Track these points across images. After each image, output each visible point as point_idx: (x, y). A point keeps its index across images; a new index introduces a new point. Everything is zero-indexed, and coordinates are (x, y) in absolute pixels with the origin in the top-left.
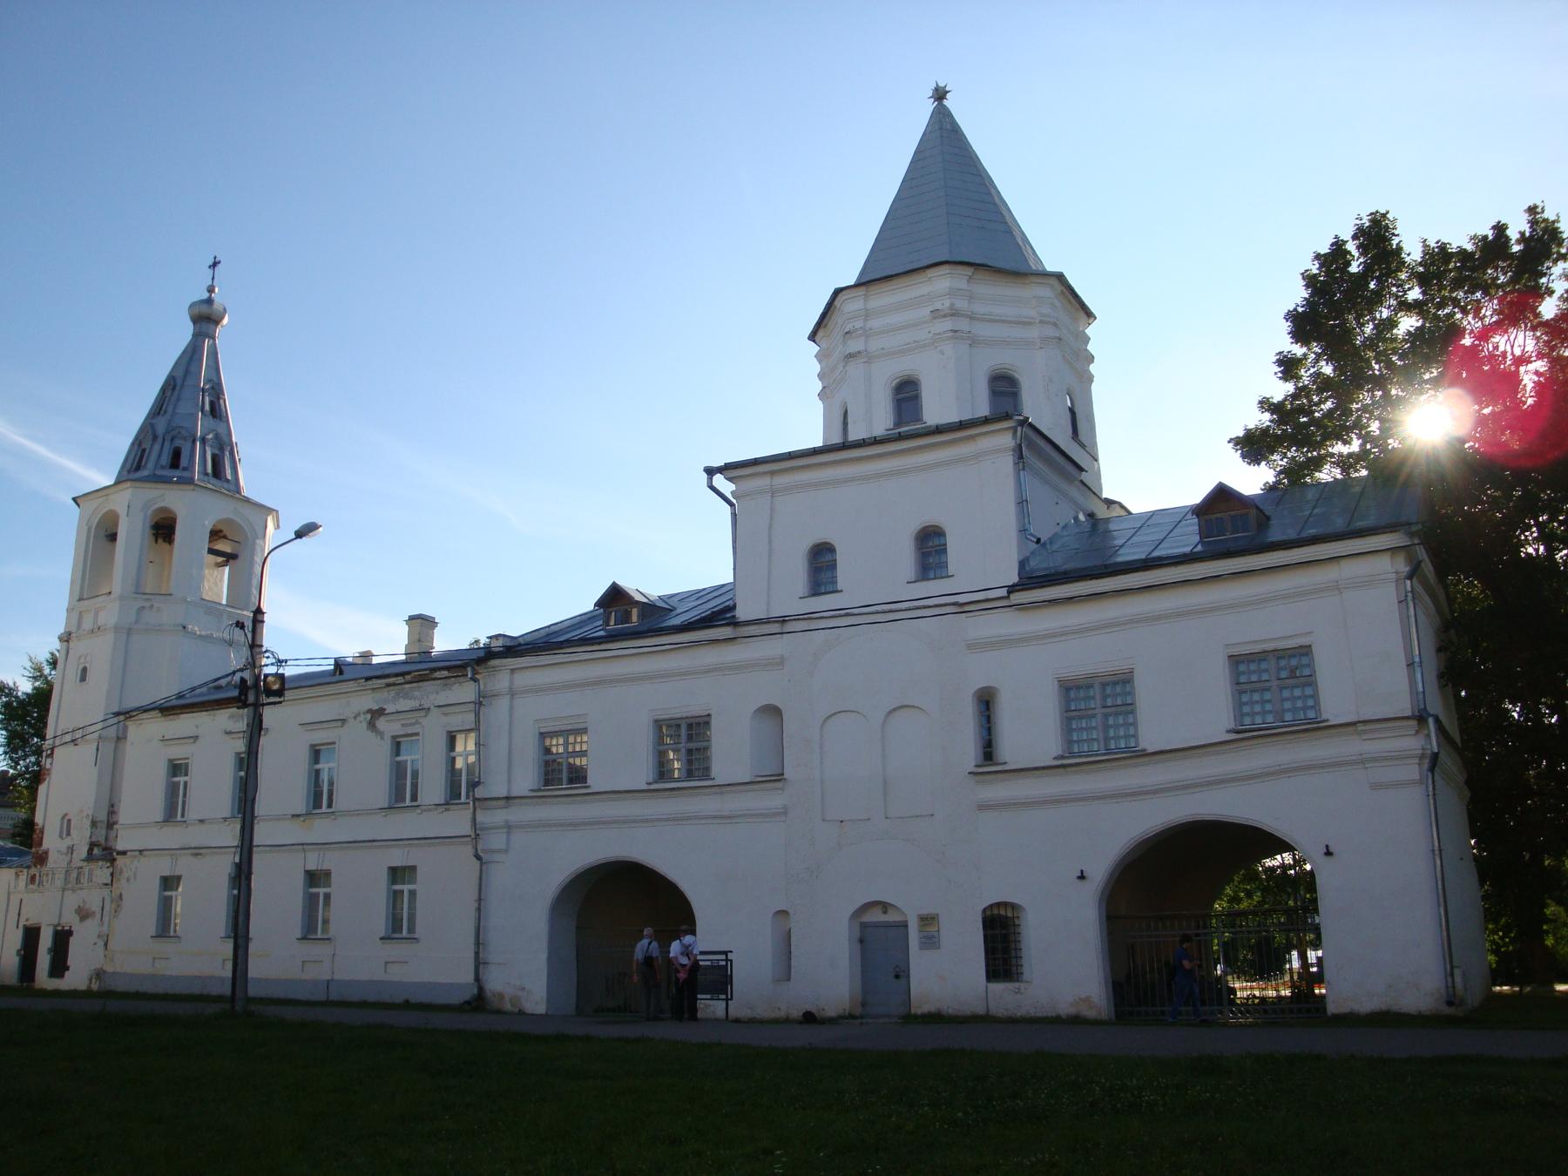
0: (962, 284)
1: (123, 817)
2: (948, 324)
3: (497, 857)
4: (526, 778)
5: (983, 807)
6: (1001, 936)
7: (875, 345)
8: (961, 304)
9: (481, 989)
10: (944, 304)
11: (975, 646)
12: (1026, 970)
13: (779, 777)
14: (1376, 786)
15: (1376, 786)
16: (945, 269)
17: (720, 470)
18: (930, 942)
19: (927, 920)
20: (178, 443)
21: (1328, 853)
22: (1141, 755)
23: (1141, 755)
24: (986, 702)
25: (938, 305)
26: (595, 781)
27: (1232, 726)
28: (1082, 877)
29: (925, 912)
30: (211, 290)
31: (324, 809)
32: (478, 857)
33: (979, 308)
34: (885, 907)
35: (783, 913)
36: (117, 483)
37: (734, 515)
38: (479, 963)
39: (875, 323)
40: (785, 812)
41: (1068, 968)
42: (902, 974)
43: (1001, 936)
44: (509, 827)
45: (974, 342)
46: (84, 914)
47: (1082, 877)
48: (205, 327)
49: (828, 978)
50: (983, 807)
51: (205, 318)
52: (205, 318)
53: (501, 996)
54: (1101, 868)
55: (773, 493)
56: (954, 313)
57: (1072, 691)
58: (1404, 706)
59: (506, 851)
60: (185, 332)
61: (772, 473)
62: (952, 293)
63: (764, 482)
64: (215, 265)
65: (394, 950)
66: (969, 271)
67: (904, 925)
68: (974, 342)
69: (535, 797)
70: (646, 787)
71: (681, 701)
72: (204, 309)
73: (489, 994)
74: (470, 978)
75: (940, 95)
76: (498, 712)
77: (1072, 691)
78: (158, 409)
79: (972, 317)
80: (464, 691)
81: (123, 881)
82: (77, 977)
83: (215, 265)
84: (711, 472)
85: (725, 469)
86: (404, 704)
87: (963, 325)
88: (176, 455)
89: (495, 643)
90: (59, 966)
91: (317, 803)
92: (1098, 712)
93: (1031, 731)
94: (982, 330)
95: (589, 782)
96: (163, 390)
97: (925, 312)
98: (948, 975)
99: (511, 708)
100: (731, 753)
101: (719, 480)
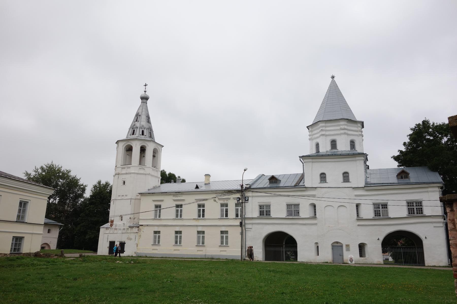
0: (346, 123)
4: (256, 214)
5: (358, 225)
7: (328, 133)
8: (346, 127)
14: (434, 227)
15: (434, 227)
19: (348, 246)
22: (390, 218)
24: (358, 206)
25: (341, 127)
26: (273, 215)
28: (379, 239)
29: (347, 244)
30: (145, 92)
31: (201, 217)
33: (349, 128)
34: (337, 242)
35: (317, 243)
41: (376, 256)
42: (342, 255)
44: (252, 224)
45: (348, 134)
46: (130, 239)
47: (379, 239)
48: (145, 101)
49: (326, 256)
50: (358, 225)
54: (382, 239)
61: (312, 159)
63: (311, 160)
66: (347, 120)
67: (342, 246)
68: (348, 134)
70: (284, 217)
75: (333, 77)
81: (142, 232)
83: (146, 85)
84: (300, 157)
87: (346, 131)
88: (143, 132)
92: (381, 210)
93: (368, 211)
95: (271, 215)
97: (338, 128)
98: (351, 256)
100: (305, 211)
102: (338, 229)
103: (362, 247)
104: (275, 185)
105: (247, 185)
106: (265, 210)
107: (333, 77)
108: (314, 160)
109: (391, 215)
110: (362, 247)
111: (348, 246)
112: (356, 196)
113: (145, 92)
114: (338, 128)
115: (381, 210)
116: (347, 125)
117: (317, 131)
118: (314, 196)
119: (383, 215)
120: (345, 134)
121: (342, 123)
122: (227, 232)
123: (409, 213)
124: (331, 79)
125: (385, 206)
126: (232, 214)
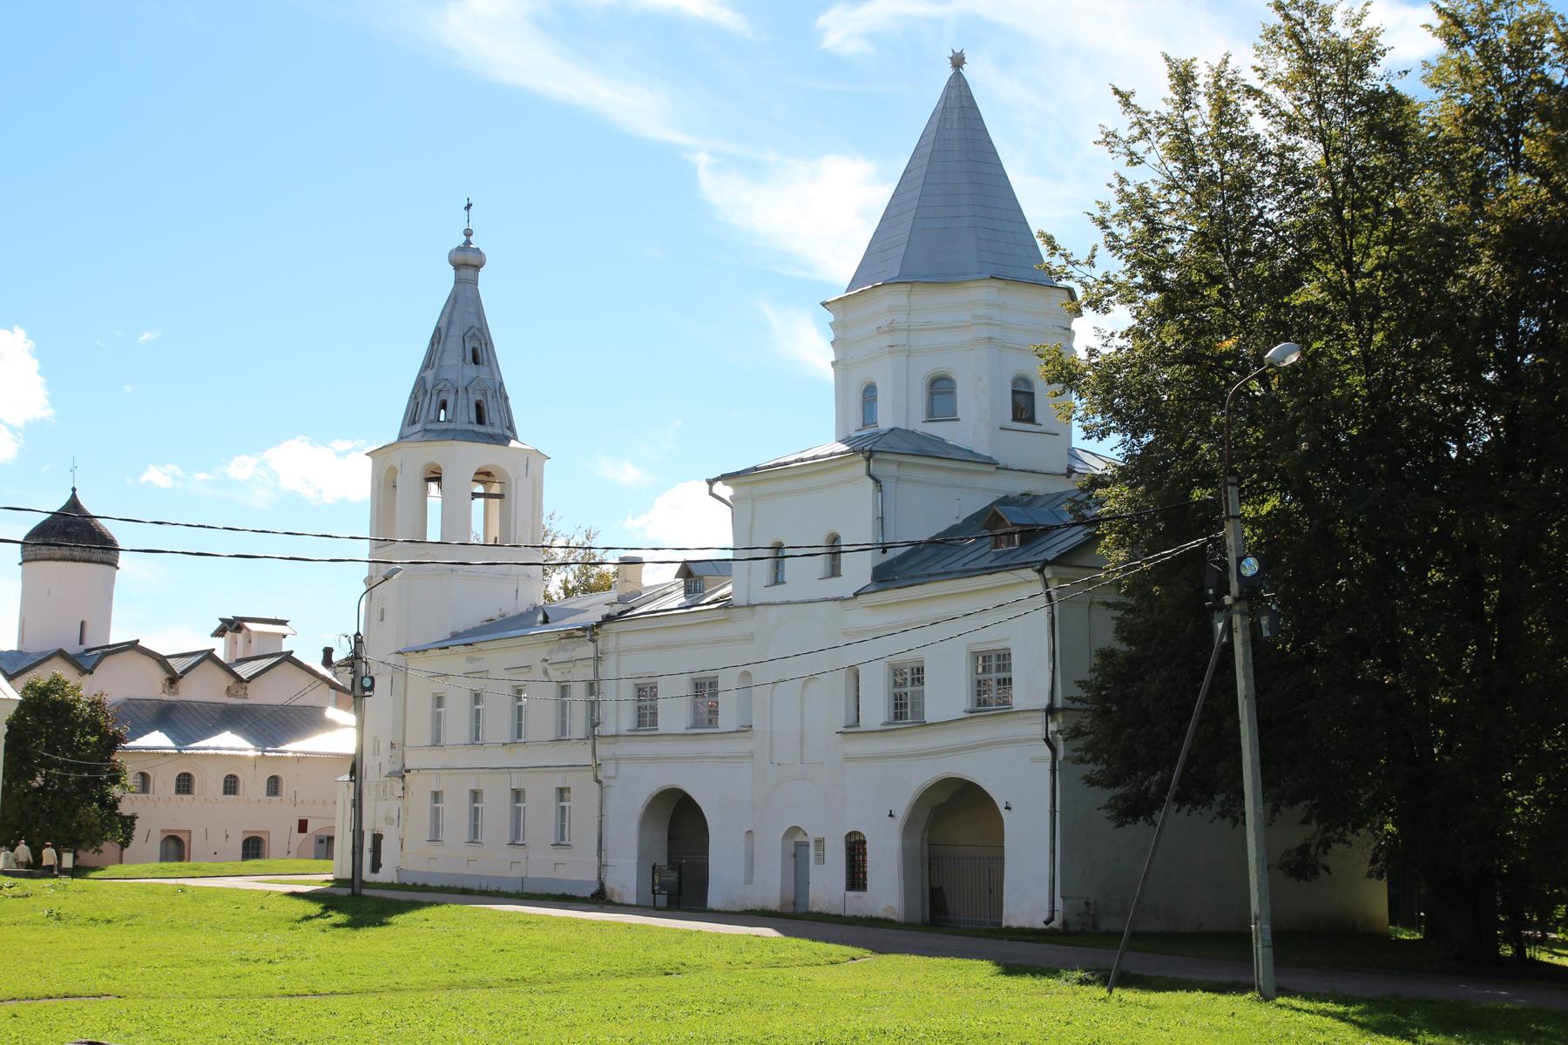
1: (408, 743)
2: (887, 340)
4: (627, 721)
5: (848, 759)
9: (602, 885)
12: (869, 883)
13: (746, 729)
17: (717, 479)
18: (821, 859)
19: (820, 842)
20: (443, 396)
23: (925, 724)
27: (969, 707)
29: (819, 836)
30: (468, 233)
35: (749, 832)
36: (401, 438)
38: (602, 867)
44: (617, 760)
50: (848, 759)
51: (467, 263)
52: (467, 263)
53: (613, 891)
54: (902, 811)
56: (892, 329)
58: (1044, 702)
60: (446, 279)
64: (468, 207)
65: (560, 855)
67: (807, 845)
69: (632, 735)
72: (461, 258)
73: (608, 891)
74: (595, 878)
75: (958, 61)
76: (608, 669)
78: (428, 364)
80: (587, 650)
82: (386, 875)
83: (468, 207)
84: (711, 482)
85: (725, 478)
86: (562, 656)
90: (376, 866)
92: (906, 689)
96: (432, 344)
99: (618, 663)
101: (719, 488)
103: (856, 848)
110: (856, 848)
111: (820, 842)
113: (468, 233)
115: (906, 689)
118: (751, 638)
126: (578, 727)
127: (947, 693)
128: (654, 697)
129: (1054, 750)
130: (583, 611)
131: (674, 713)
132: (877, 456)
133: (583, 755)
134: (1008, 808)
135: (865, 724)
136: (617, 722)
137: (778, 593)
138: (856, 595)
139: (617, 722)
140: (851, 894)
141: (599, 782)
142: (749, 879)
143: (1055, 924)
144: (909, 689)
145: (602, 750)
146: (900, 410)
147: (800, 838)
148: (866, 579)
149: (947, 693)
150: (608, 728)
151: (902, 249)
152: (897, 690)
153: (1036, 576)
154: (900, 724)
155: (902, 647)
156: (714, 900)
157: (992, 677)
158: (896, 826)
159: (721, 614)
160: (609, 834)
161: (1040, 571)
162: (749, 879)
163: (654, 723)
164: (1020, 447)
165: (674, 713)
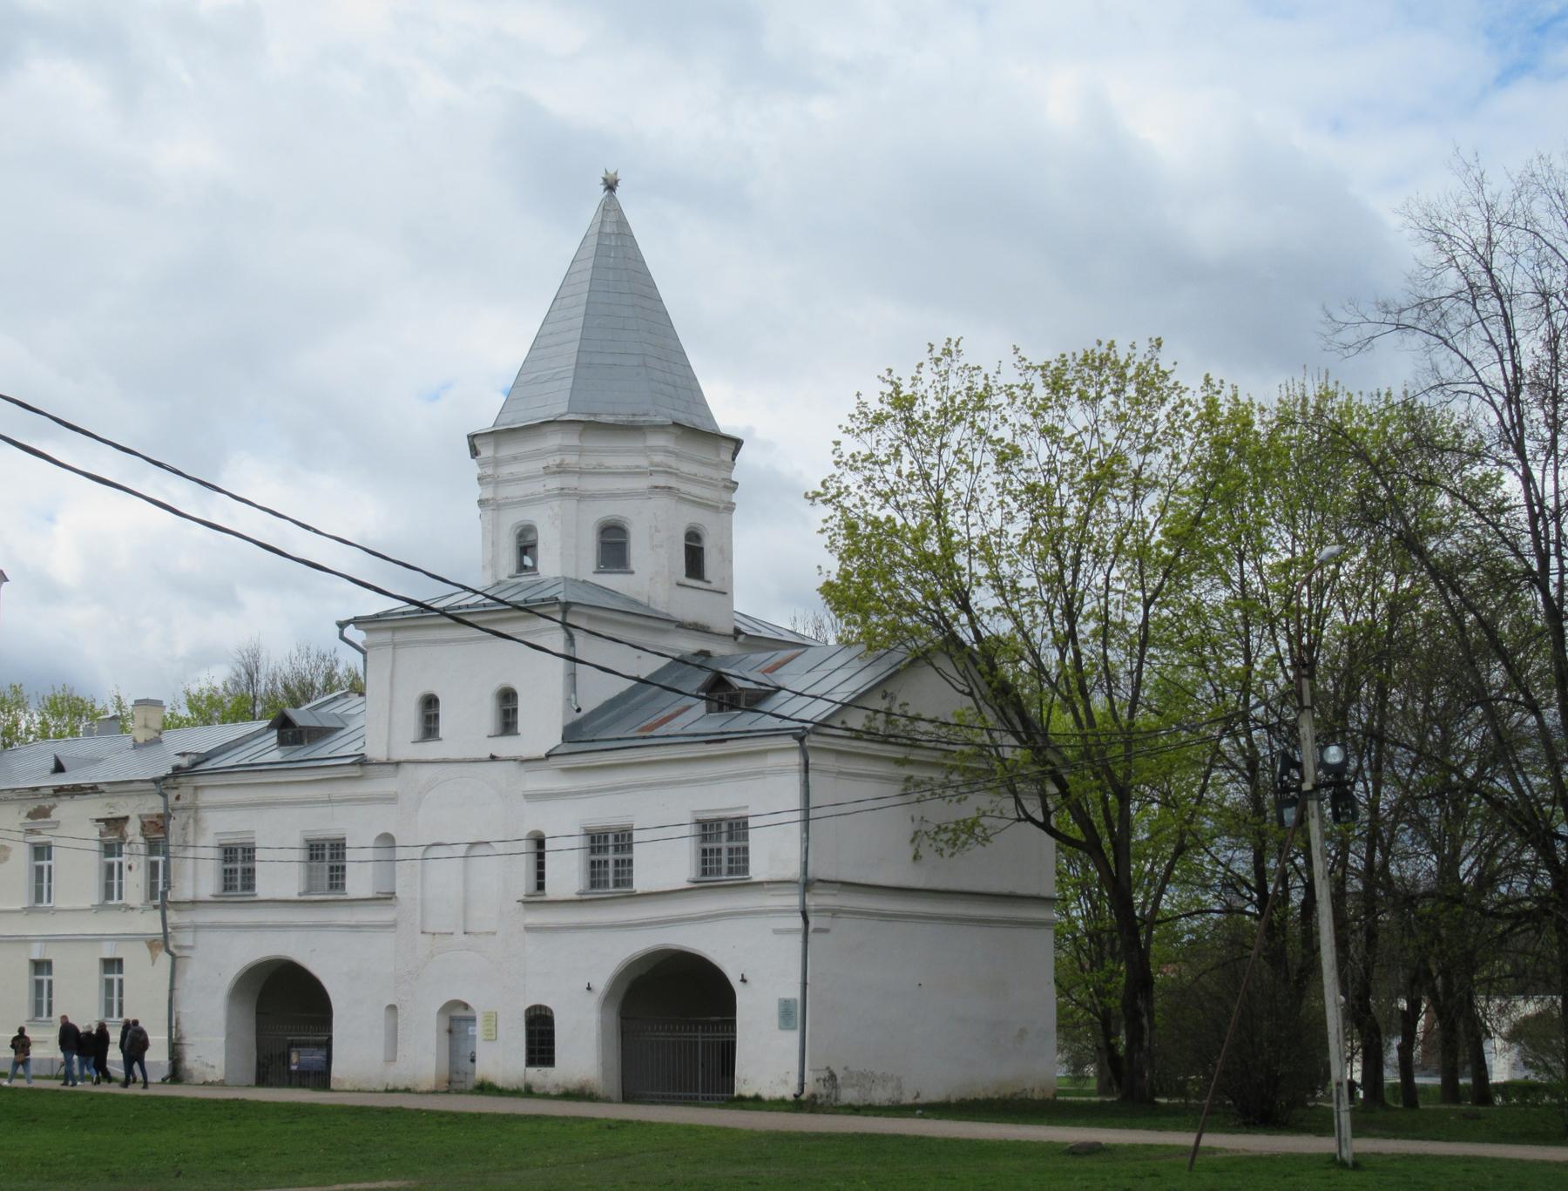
2: (554, 483)
3: (186, 953)
6: (540, 1035)
8: (571, 459)
10: (553, 461)
11: (530, 797)
13: (387, 898)
14: (776, 932)
15: (776, 932)
16: (557, 427)
17: (348, 622)
18: (492, 1037)
21: (744, 980)
32: (168, 951)
33: (590, 461)
35: (392, 1008)
37: (365, 661)
39: (505, 471)
40: (392, 925)
43: (540, 1035)
44: (196, 928)
45: (581, 497)
49: (421, 1061)
54: (601, 982)
55: (395, 645)
56: (561, 470)
57: (597, 840)
58: (793, 870)
59: (191, 948)
61: (394, 629)
62: (561, 450)
63: (386, 637)
67: (473, 1020)
68: (581, 497)
70: (295, 897)
71: (325, 824)
75: (611, 186)
77: (597, 840)
79: (581, 473)
84: (342, 625)
85: (357, 621)
87: (571, 482)
89: (184, 762)
91: (39, 898)
93: (567, 873)
94: (591, 484)
97: (537, 466)
101: (351, 632)
102: (462, 950)
104: (301, 753)
105: (183, 754)
106: (239, 866)
107: (611, 186)
108: (400, 637)
109: (640, 883)
111: (492, 1018)
112: (530, 797)
114: (537, 466)
116: (581, 452)
117: (527, 462)
118: (391, 799)
119: (617, 884)
120: (562, 493)
121: (554, 440)
122: (120, 961)
123: (704, 872)
124: (600, 193)
125: (623, 839)
127: (664, 862)
128: (252, 859)
129: (806, 922)
130: (95, 761)
131: (280, 876)
132: (574, 608)
133: (150, 923)
134: (744, 980)
135: (553, 890)
136: (195, 886)
137: (431, 750)
138: (548, 756)
139: (195, 886)
140: (533, 1071)
141: (172, 954)
142: (391, 1057)
143: (804, 1097)
144: (611, 857)
145: (173, 917)
146: (564, 558)
147: (461, 1013)
148: (554, 739)
149: (664, 862)
150: (184, 889)
151: (569, 383)
152: (595, 857)
153: (796, 744)
154: (600, 892)
155: (607, 812)
156: (333, 1086)
157: (722, 849)
158: (592, 1004)
159: (356, 771)
160: (185, 1008)
161: (801, 740)
162: (391, 1057)
163: (249, 885)
164: (690, 604)
165: (280, 876)
